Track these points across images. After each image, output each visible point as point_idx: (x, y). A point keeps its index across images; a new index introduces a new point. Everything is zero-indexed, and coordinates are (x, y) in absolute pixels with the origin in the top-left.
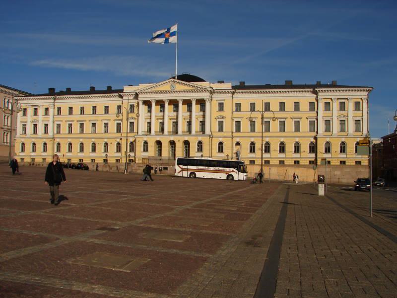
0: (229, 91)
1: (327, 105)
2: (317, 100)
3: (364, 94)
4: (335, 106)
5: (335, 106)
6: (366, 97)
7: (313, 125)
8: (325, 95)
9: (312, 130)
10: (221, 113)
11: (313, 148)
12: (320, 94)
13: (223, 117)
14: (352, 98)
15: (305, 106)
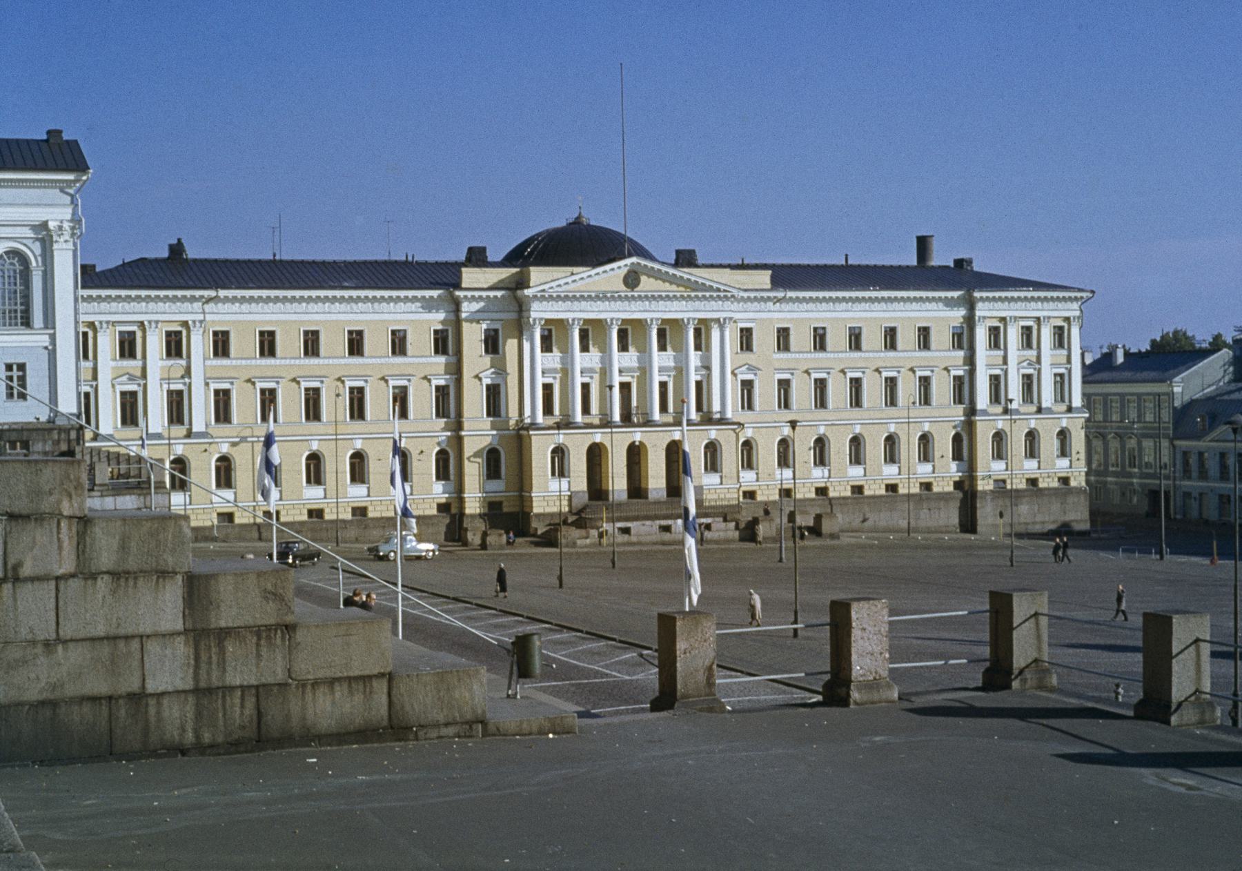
0: (765, 295)
1: (994, 331)
2: (970, 321)
3: (1073, 310)
4: (1013, 336)
5: (1013, 336)
6: (1078, 313)
7: (963, 389)
8: (989, 310)
9: (959, 399)
10: (747, 357)
11: (963, 446)
12: (979, 305)
13: (752, 369)
14: (1049, 318)
15: (941, 338)
